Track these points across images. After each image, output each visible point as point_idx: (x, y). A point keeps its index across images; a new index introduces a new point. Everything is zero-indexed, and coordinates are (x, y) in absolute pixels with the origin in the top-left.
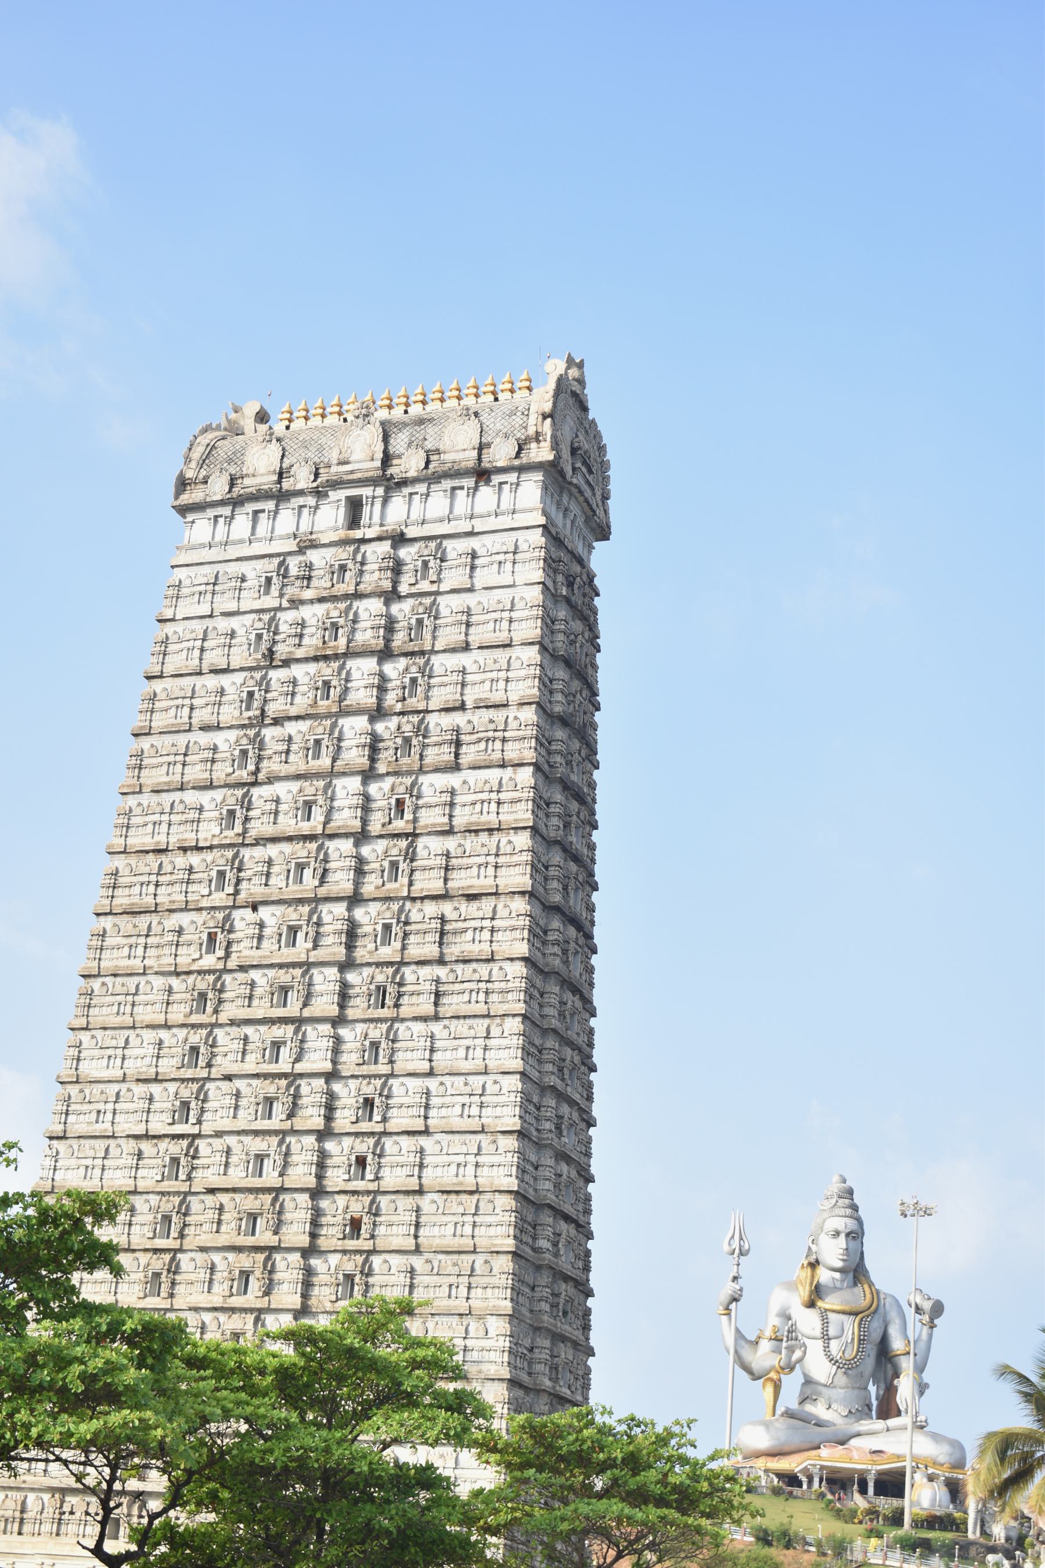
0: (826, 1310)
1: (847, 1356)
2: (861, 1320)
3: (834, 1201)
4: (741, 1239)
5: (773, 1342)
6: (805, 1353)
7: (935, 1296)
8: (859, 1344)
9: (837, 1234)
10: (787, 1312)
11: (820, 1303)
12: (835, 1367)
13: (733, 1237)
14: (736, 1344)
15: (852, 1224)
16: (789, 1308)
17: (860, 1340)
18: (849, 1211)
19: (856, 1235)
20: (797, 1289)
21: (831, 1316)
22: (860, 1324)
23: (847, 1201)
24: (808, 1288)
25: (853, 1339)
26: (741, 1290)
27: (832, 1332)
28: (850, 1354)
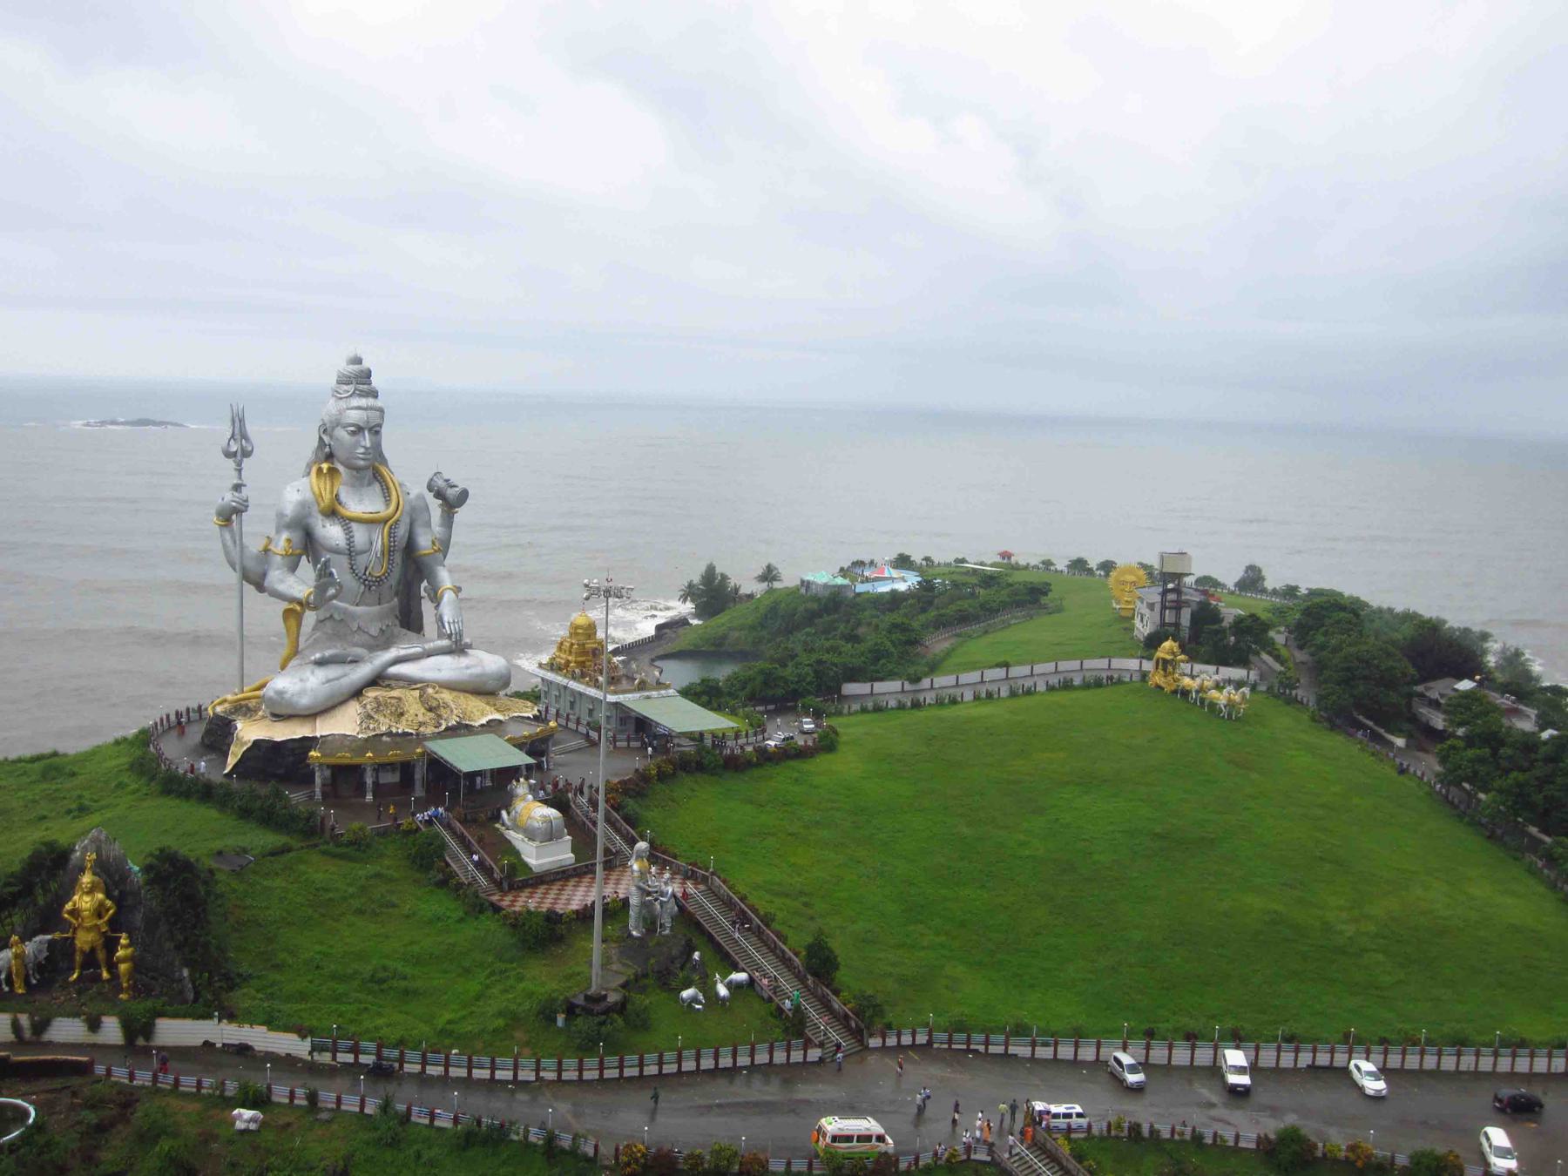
0: (352, 520)
21: (354, 526)
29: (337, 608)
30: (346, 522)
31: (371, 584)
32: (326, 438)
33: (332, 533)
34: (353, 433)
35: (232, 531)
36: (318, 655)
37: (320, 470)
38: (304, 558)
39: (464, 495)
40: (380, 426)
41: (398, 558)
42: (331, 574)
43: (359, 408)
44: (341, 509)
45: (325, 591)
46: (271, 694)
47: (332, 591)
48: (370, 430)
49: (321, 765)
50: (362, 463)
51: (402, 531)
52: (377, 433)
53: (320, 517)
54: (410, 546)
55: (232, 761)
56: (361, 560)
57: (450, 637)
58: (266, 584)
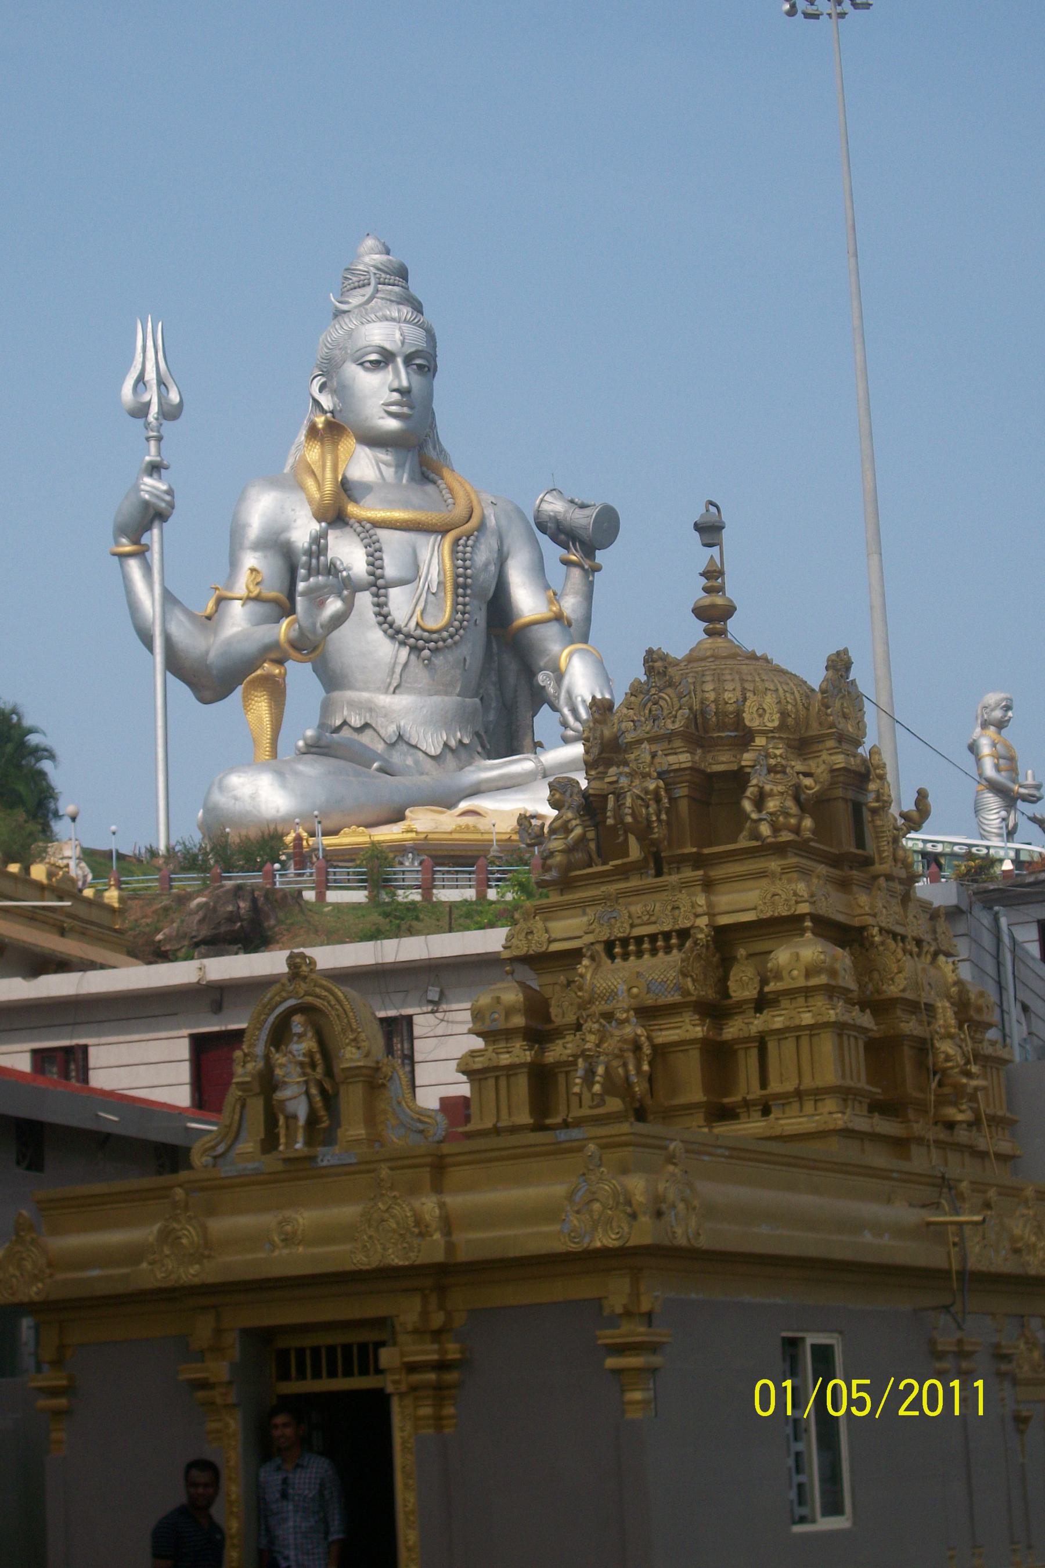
0: (377, 524)
2: (456, 542)
3: (369, 291)
4: (161, 382)
5: (251, 605)
7: (598, 500)
10: (283, 537)
13: (141, 379)
15: (416, 338)
16: (286, 528)
17: (456, 586)
18: (406, 311)
19: (423, 362)
20: (302, 487)
21: (383, 534)
22: (454, 552)
24: (329, 475)
26: (170, 492)
27: (391, 571)
28: (439, 618)
29: (352, 705)
30: (369, 531)
31: (418, 643)
34: (376, 365)
35: (147, 569)
39: (608, 525)
42: (332, 569)
43: (386, 319)
44: (352, 509)
45: (322, 604)
48: (408, 360)
50: (392, 424)
51: (483, 555)
56: (400, 604)
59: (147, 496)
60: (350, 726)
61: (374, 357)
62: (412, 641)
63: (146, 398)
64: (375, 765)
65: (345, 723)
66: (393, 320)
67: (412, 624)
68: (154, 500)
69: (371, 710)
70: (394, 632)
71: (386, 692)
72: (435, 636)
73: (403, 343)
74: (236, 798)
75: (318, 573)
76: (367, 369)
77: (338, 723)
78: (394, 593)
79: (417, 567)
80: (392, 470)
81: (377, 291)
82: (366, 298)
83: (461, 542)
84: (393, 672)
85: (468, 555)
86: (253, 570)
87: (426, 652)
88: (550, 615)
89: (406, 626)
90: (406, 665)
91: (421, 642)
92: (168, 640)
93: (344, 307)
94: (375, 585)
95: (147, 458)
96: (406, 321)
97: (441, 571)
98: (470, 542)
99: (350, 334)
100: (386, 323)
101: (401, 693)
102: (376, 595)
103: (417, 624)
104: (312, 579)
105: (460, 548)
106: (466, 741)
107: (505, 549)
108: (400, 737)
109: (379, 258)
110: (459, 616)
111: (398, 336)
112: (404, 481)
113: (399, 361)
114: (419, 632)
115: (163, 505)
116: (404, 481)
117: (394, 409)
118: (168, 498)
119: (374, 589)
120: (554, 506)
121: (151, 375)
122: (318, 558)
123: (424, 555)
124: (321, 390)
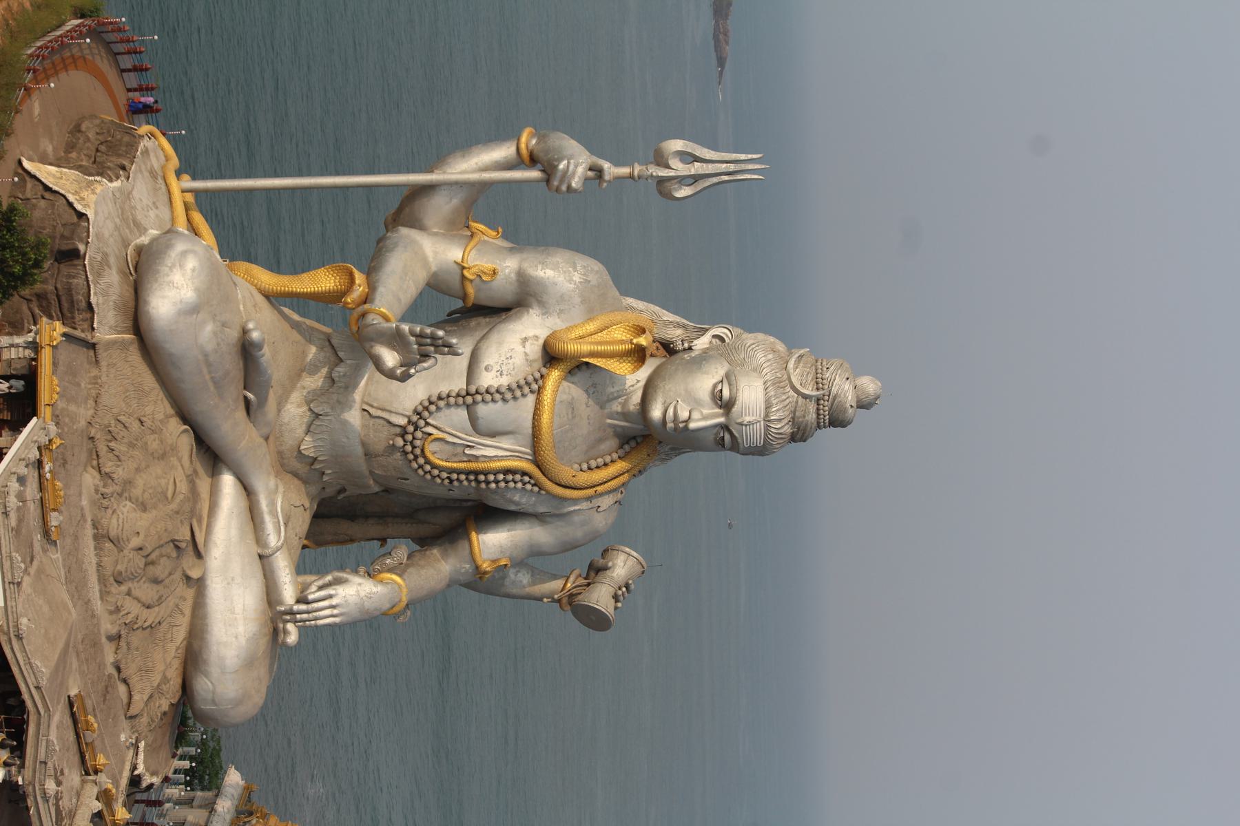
1: (430, 448)
2: (524, 474)
4: (696, 178)
6: (390, 374)
8: (468, 473)
9: (727, 406)
10: (532, 300)
11: (555, 375)
12: (402, 421)
13: (697, 159)
14: (456, 184)
16: (542, 304)
17: (476, 473)
21: (531, 399)
23: (811, 416)
24: (585, 348)
25: (476, 458)
26: (558, 190)
32: (702, 343)
33: (510, 350)
34: (717, 397)
36: (255, 335)
37: (641, 331)
38: (459, 304)
40: (735, 446)
41: (464, 488)
43: (768, 406)
46: (180, 247)
47: (390, 358)
48: (725, 427)
49: (35, 346)
50: (656, 413)
51: (520, 498)
52: (720, 443)
53: (543, 334)
54: (488, 513)
55: (48, 173)
57: (301, 600)
58: (404, 231)
59: (561, 166)
60: (336, 365)
61: (726, 393)
62: (411, 429)
63: (675, 163)
64: (250, 396)
65: (341, 361)
66: (767, 415)
67: (429, 429)
68: (559, 175)
69: (346, 388)
70: (422, 412)
71: (363, 402)
72: (418, 451)
73: (741, 424)
74: (171, 268)
75: (420, 345)
76: (715, 386)
77: (341, 354)
78: (463, 413)
79: (493, 435)
80: (619, 409)
81: (805, 397)
82: (798, 386)
83: (526, 479)
84: (383, 410)
85: (512, 485)
86: (494, 272)
87: (400, 442)
88: (480, 563)
89: (427, 424)
90: (389, 422)
91: (409, 437)
92: (429, 188)
93: (791, 365)
94: (468, 394)
95: (606, 165)
96: (767, 427)
97: (491, 459)
98: (529, 487)
99: (758, 370)
100: (763, 407)
101: (363, 417)
102: (458, 395)
103: (430, 434)
104: (413, 339)
105: (518, 477)
106: (325, 478)
107: (549, 519)
108: (317, 415)
109: (849, 398)
110: (445, 475)
111: (747, 419)
112: (609, 421)
113: (722, 420)
114: (419, 434)
115: (556, 183)
116: (609, 421)
117: (671, 412)
118: (564, 188)
119: (464, 393)
120: (622, 566)
121: (697, 168)
122: (432, 345)
123: (505, 443)
124: (715, 336)
